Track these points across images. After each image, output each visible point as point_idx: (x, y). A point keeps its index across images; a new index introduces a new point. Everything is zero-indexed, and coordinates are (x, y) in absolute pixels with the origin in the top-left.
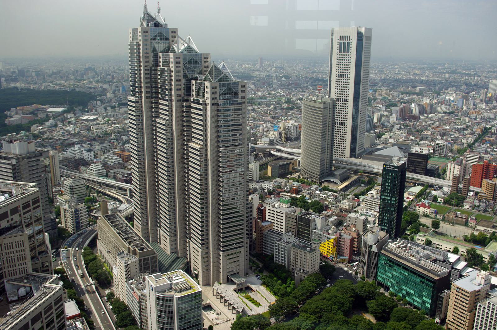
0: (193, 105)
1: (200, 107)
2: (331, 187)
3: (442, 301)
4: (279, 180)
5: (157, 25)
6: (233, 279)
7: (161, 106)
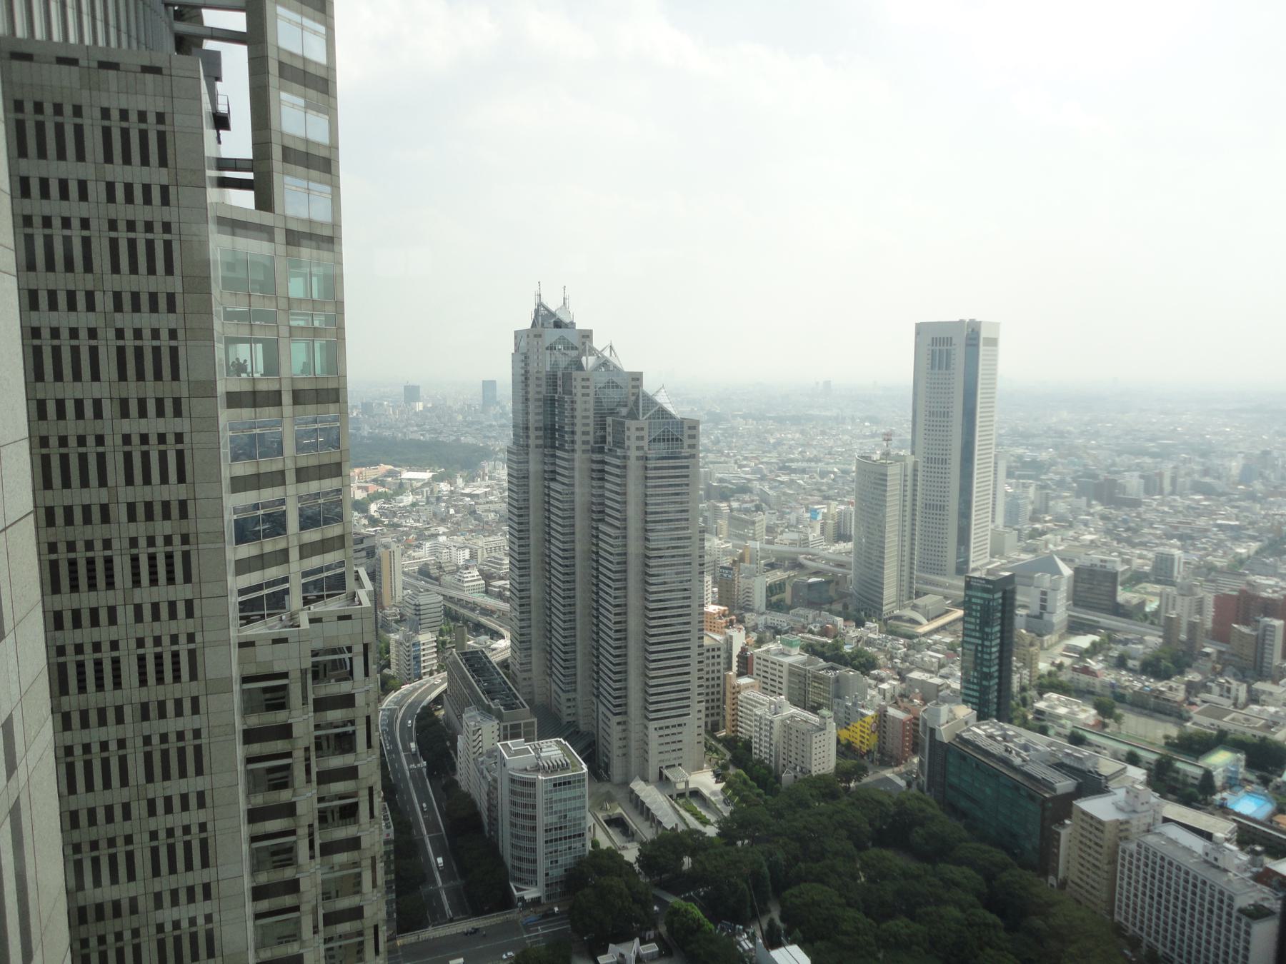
0: (608, 459)
1: (618, 462)
2: (906, 627)
3: (1058, 840)
4: (801, 611)
5: (558, 324)
6: (670, 776)
7: (558, 462)
